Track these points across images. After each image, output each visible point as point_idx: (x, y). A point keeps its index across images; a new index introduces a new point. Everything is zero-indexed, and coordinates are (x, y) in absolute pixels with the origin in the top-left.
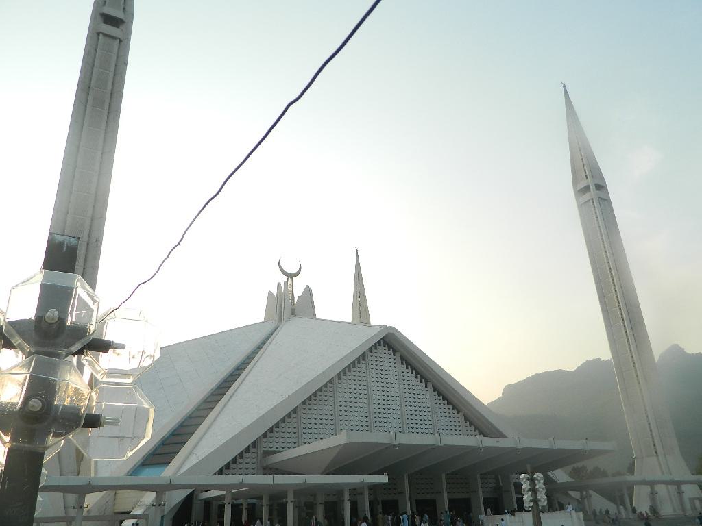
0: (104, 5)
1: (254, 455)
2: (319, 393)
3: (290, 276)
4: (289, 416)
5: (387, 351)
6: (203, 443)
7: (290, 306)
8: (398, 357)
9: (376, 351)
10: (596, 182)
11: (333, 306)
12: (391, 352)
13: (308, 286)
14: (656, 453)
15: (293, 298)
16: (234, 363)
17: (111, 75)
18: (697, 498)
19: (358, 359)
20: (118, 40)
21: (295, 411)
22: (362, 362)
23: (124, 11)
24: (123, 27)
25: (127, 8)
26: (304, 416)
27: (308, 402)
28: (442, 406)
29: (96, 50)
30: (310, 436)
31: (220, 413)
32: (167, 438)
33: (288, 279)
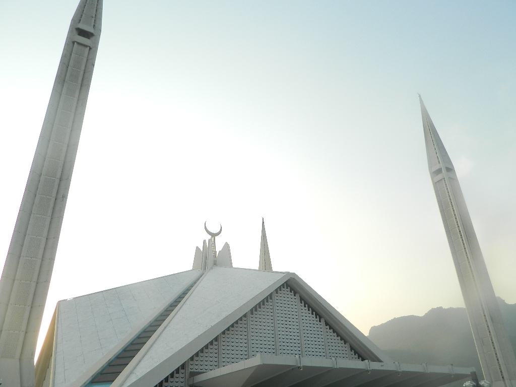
0: (79, 22)
2: (235, 325)
3: (213, 235)
4: (211, 343)
5: (289, 293)
8: (297, 296)
11: (245, 258)
12: (292, 293)
14: (503, 377)
15: (216, 252)
17: (82, 73)
20: (88, 48)
21: (216, 339)
22: (270, 300)
24: (93, 38)
25: (96, 25)
26: (224, 344)
27: (227, 332)
28: (332, 337)
29: (71, 55)
30: (237, 356)
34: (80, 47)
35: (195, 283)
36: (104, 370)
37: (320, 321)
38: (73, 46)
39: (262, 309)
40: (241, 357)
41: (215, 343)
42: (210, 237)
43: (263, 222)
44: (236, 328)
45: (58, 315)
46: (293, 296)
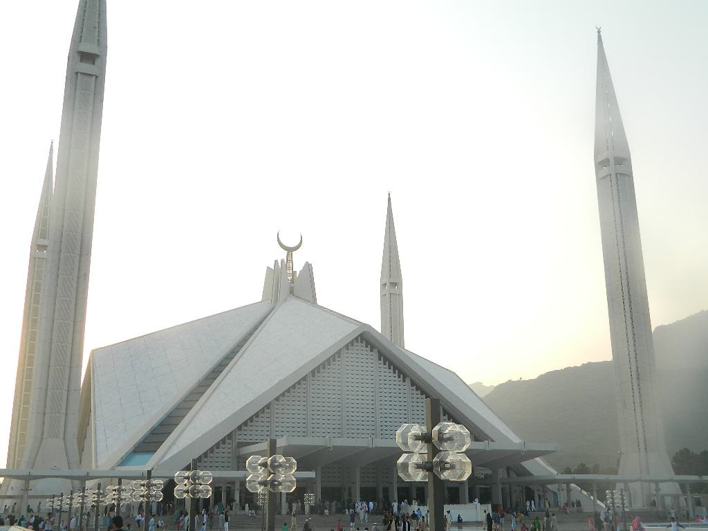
0: (80, 41)
1: (230, 446)
3: (290, 250)
4: (262, 410)
5: (364, 348)
7: (291, 285)
8: (375, 354)
9: (352, 348)
12: (369, 348)
13: (307, 262)
15: (294, 273)
16: (229, 343)
18: (669, 495)
19: (333, 356)
22: (337, 359)
27: (281, 398)
32: (155, 429)
33: (288, 254)
34: (86, 78)
35: (260, 323)
37: (404, 381)
38: (77, 78)
41: (266, 411)
42: (283, 255)
43: (389, 200)
44: (299, 387)
46: (369, 352)
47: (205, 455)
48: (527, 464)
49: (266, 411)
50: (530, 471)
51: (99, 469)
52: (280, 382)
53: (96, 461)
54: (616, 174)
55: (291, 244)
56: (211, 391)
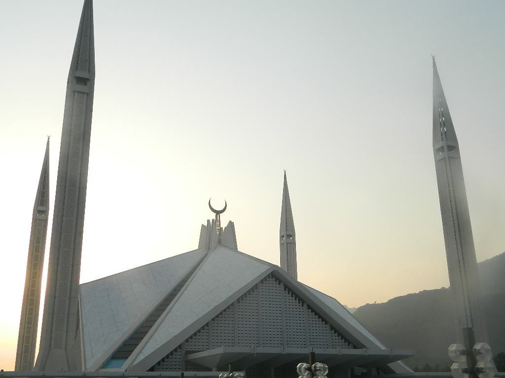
0: (77, 69)
1: (179, 353)
3: (218, 213)
4: (203, 328)
6: (148, 346)
7: (218, 237)
8: (282, 286)
9: (266, 282)
10: (448, 145)
21: (207, 325)
22: (255, 290)
23: (89, 72)
24: (88, 84)
28: (314, 319)
31: (160, 325)
32: (127, 341)
35: (198, 264)
36: (120, 349)
38: (74, 95)
39: (216, 321)
40: (217, 344)
41: (206, 328)
42: (213, 216)
45: (80, 300)
46: (277, 285)
47: (163, 360)
48: (392, 365)
49: (206, 328)
50: (395, 370)
51: (87, 371)
52: (216, 306)
53: (85, 365)
54: (449, 158)
55: (219, 208)
56: (166, 314)
